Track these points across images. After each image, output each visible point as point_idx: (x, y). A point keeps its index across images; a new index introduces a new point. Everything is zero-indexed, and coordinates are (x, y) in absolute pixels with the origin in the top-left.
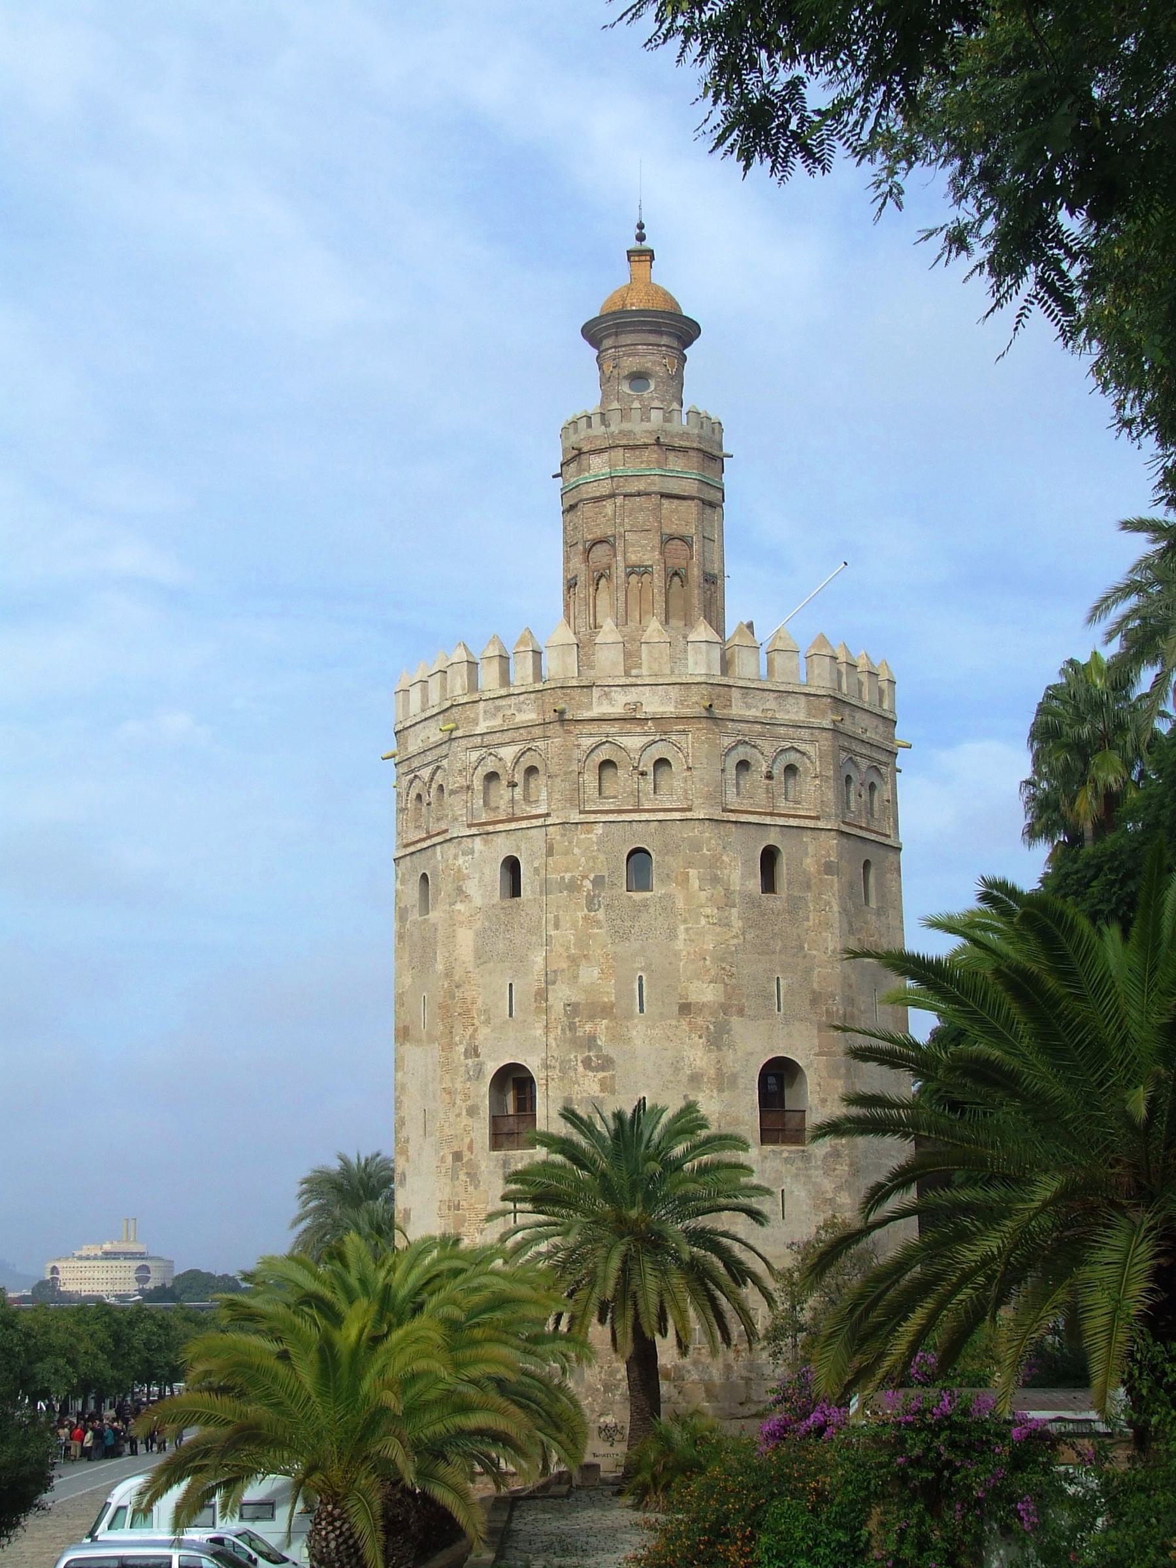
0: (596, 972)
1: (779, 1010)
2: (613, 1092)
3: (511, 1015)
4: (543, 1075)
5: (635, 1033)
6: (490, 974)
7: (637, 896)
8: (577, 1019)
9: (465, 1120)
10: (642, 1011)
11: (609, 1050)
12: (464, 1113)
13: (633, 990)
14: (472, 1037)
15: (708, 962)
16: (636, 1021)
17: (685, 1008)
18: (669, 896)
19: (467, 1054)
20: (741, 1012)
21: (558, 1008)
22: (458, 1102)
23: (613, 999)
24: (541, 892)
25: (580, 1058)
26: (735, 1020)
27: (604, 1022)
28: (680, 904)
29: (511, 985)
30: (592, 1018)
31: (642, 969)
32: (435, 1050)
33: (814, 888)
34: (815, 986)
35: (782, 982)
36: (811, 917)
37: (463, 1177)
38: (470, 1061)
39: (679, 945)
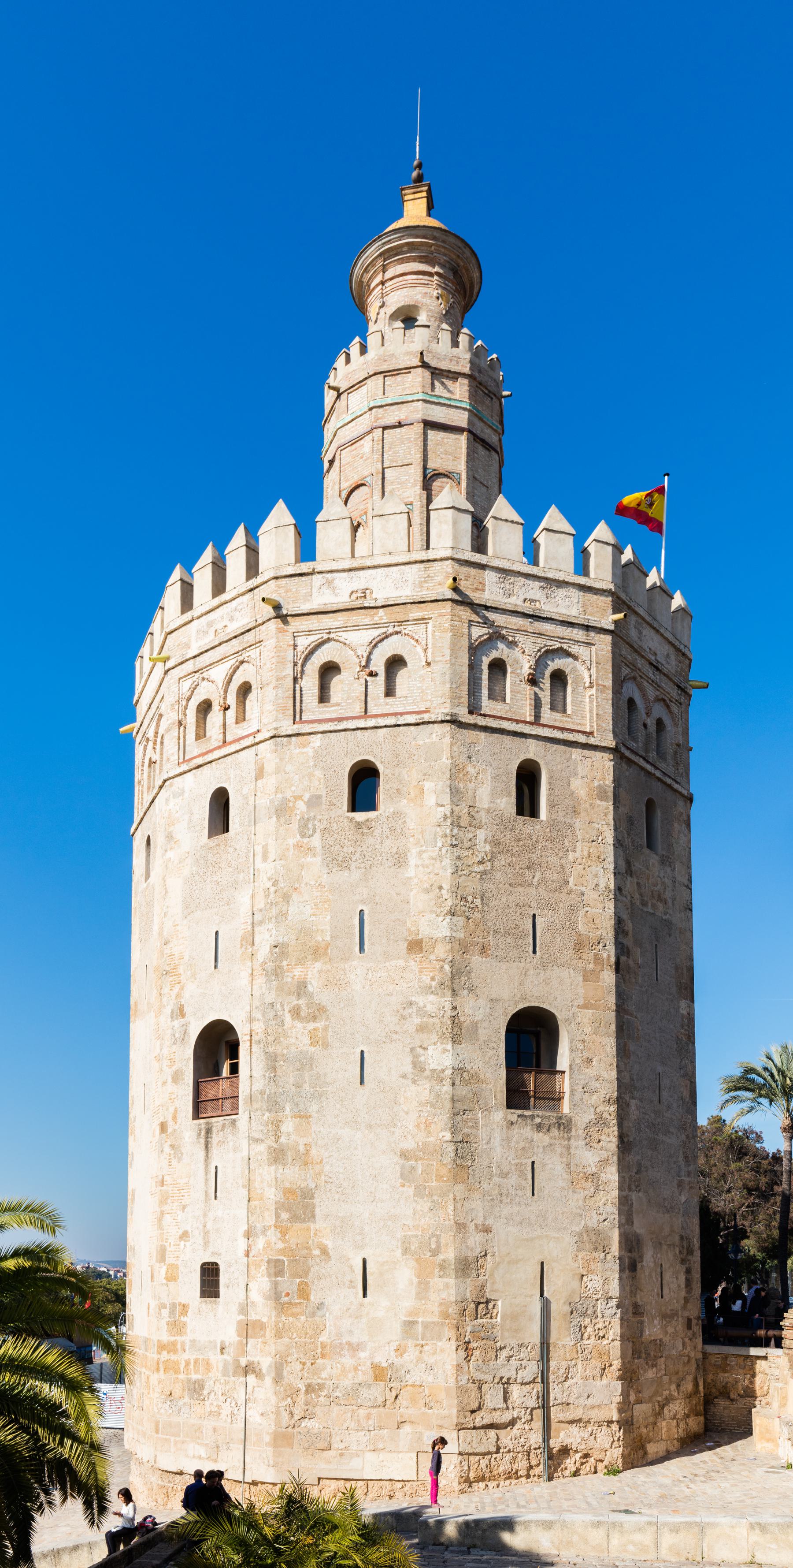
0: (308, 909)
1: (534, 952)
2: (326, 1045)
5: (353, 977)
7: (360, 816)
8: (285, 963)
10: (362, 949)
11: (324, 998)
13: (352, 927)
15: (444, 892)
16: (355, 963)
17: (415, 946)
18: (397, 815)
20: (483, 950)
21: (263, 951)
23: (328, 938)
25: (287, 1008)
26: (476, 960)
27: (318, 965)
28: (411, 825)
30: (301, 961)
31: (363, 902)
33: (583, 814)
34: (581, 928)
35: (538, 920)
36: (579, 849)
39: (411, 872)
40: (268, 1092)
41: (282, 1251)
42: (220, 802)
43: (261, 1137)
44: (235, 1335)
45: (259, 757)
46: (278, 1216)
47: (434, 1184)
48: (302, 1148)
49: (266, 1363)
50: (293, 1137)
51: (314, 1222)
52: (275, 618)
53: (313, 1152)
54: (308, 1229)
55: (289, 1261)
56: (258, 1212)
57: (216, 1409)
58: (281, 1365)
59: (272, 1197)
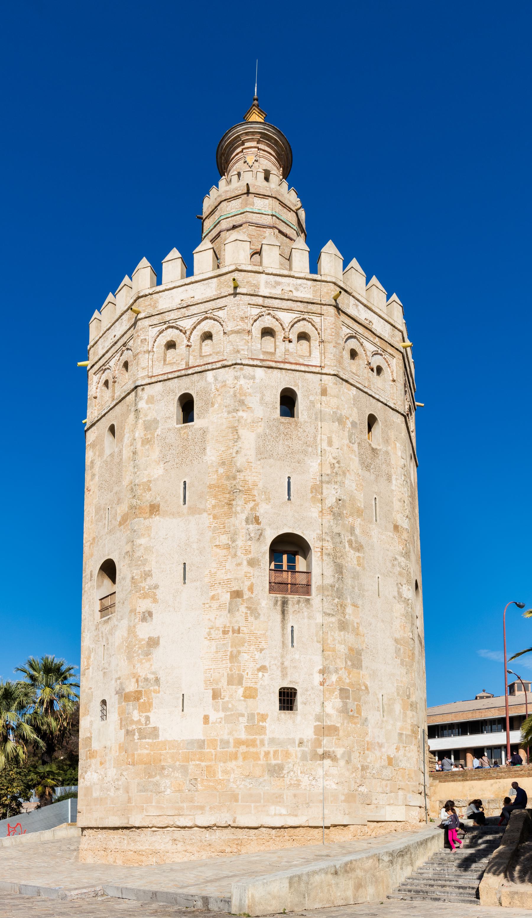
3: (289, 499)
4: (319, 544)
6: (271, 467)
9: (245, 567)
12: (245, 563)
14: (252, 509)
19: (247, 521)
22: (239, 553)
24: (316, 418)
29: (289, 478)
32: (206, 519)
37: (243, 609)
38: (251, 527)
40: (337, 586)
41: (351, 684)
42: (288, 401)
43: (332, 612)
44: (313, 734)
45: (323, 382)
46: (346, 663)
47: (407, 660)
48: (355, 625)
49: (339, 752)
50: (352, 617)
51: (362, 670)
52: (334, 306)
53: (360, 628)
54: (359, 673)
55: (353, 691)
56: (331, 658)
57: (296, 782)
58: (350, 753)
59: (342, 650)
